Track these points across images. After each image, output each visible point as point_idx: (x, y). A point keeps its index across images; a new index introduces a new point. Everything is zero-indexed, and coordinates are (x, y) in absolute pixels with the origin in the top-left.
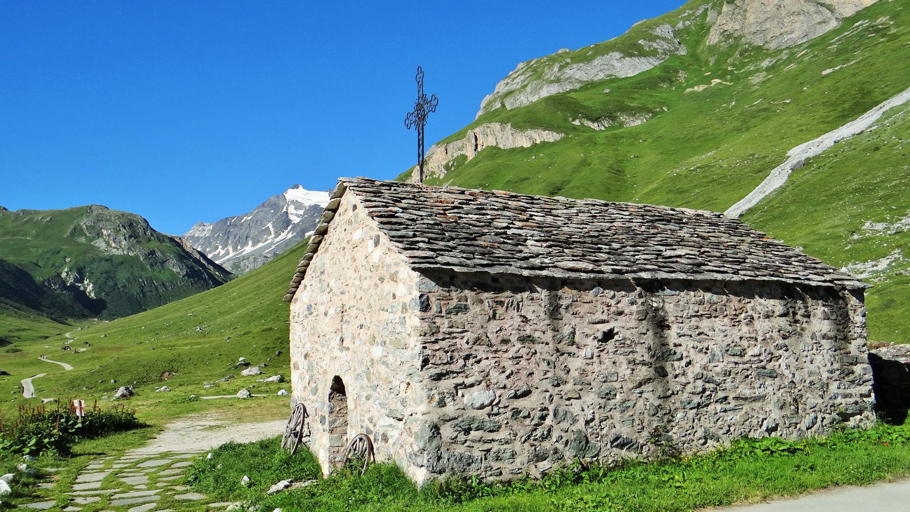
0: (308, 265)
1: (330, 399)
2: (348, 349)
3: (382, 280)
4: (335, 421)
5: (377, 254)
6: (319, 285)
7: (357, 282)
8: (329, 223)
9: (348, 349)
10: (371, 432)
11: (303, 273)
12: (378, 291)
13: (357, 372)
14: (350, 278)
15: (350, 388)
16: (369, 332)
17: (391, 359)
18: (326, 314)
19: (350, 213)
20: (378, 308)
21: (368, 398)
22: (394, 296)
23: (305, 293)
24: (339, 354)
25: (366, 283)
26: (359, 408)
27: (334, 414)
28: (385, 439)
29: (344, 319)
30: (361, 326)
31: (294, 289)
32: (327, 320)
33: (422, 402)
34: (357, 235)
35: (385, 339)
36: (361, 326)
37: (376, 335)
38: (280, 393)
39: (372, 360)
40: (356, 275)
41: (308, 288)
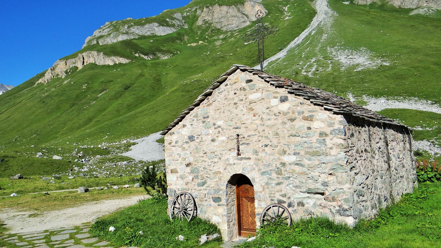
0: (188, 113)
1: (227, 187)
2: (249, 158)
3: (292, 120)
4: (228, 199)
5: (285, 107)
6: (201, 124)
7: (258, 122)
8: (213, 89)
9: (249, 158)
10: (284, 202)
11: (183, 118)
12: (287, 126)
13: (262, 171)
14: (247, 119)
15: (257, 180)
16: (277, 149)
17: (306, 162)
18: (213, 140)
19: (244, 84)
20: (288, 135)
21: (279, 184)
22: (309, 128)
23: (185, 129)
24: (236, 161)
25: (269, 123)
26: (267, 191)
27: (228, 195)
28: (301, 204)
29: (241, 143)
30: (266, 146)
31: (171, 127)
32: (216, 144)
33: (346, 182)
34: (253, 97)
35: (298, 151)
36: (266, 146)
37: (286, 149)
38: (12, 195)
39: (284, 164)
40: (255, 118)
41: (188, 126)
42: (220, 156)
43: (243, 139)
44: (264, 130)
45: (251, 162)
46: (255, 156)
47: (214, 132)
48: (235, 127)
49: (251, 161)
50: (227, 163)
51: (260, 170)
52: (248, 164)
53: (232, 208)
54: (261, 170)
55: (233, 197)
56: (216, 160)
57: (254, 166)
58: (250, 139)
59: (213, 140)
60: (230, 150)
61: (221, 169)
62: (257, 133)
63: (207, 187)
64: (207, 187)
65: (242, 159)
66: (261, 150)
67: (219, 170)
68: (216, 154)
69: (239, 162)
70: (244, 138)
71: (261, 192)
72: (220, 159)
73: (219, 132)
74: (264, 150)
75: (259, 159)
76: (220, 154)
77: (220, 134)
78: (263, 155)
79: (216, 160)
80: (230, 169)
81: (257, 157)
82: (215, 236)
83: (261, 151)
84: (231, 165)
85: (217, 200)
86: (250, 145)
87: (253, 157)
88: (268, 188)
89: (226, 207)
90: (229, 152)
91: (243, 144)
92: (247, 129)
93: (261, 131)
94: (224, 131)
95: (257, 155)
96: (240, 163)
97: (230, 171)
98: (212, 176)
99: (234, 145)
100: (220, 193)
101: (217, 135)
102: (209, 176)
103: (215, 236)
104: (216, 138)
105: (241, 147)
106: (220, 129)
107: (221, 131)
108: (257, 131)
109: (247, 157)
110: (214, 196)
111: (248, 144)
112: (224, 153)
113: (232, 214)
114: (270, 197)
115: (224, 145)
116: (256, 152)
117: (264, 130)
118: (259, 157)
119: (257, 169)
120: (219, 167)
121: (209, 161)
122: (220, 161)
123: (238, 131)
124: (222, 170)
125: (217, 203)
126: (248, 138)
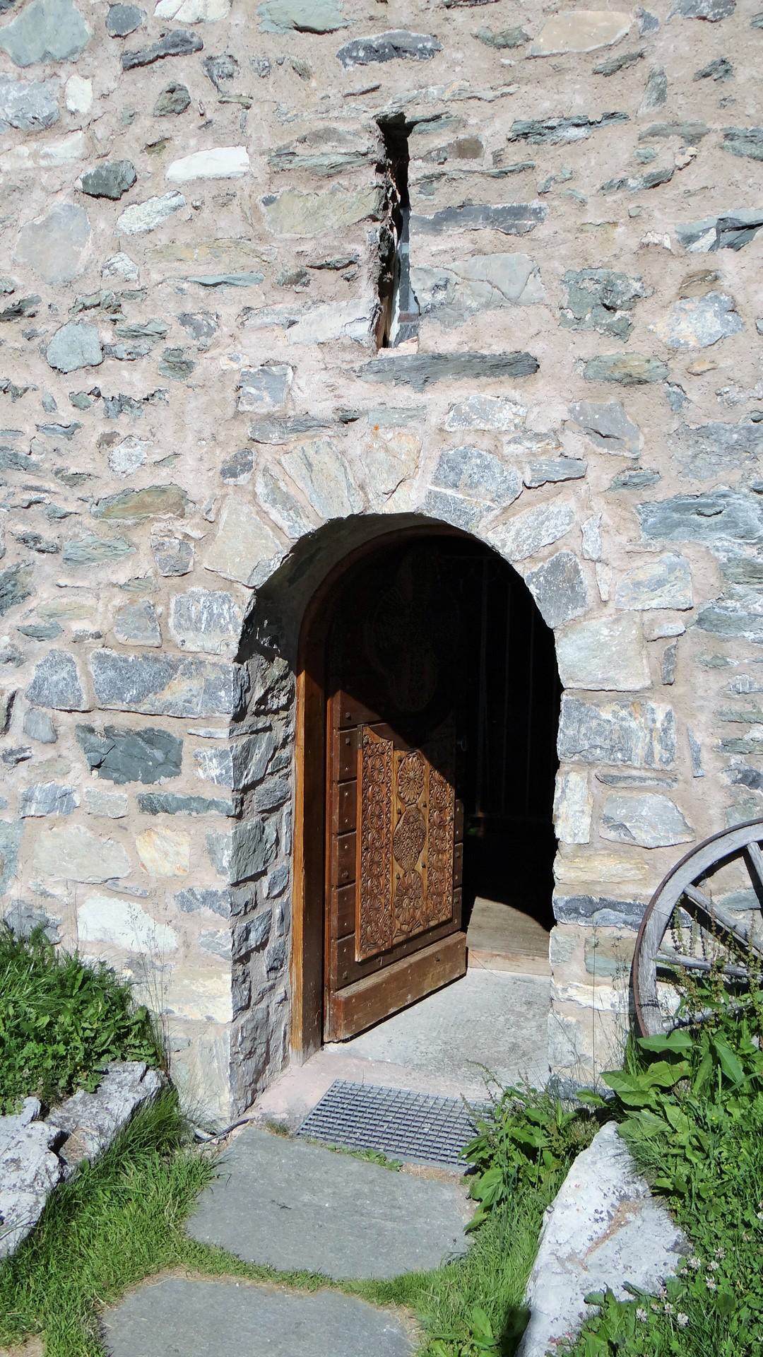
2: (520, 366)
4: (248, 750)
9: (520, 366)
13: (664, 492)
15: (601, 581)
24: (358, 394)
29: (421, 205)
42: (180, 337)
43: (454, 165)
44: (722, 69)
45: (545, 404)
46: (593, 344)
47: (117, 103)
48: (374, 37)
49: (541, 386)
50: (266, 405)
51: (632, 481)
52: (505, 416)
53: (270, 833)
54: (648, 482)
55: (279, 733)
56: (134, 380)
57: (575, 443)
58: (548, 161)
59: (106, 189)
60: (299, 278)
61: (189, 461)
62: (638, 102)
63: (35, 634)
64: (35, 634)
65: (430, 369)
66: (671, 276)
67: (162, 477)
68: (132, 317)
69: (404, 395)
70: (469, 149)
71: (633, 700)
72: (179, 365)
73: (176, 102)
74: (710, 278)
75: (637, 366)
76: (185, 319)
77: (189, 121)
78: (694, 325)
79: (134, 380)
80: (291, 464)
81: (611, 350)
82: (124, 1090)
83: (669, 288)
84: (305, 425)
85: (135, 756)
86: (543, 231)
87: (565, 350)
88: (718, 664)
89: (227, 829)
90: (287, 303)
91: (450, 215)
92: (507, 58)
93: (680, 73)
94: (235, 88)
95: (622, 332)
96: (418, 413)
97: (300, 489)
98: (85, 531)
99: (348, 231)
100: (167, 696)
101: (147, 129)
102: (49, 534)
103: (124, 1090)
104: (145, 164)
105: (421, 249)
106: (184, 70)
107: (201, 94)
108: (639, 72)
109: (497, 347)
110: (99, 721)
111: (518, 212)
112: (228, 312)
113: (265, 881)
114: (729, 745)
115: (229, 224)
116: (609, 303)
117: (722, 69)
118: (635, 353)
119: (601, 473)
120: (178, 445)
121: (59, 390)
122: (175, 387)
123: (401, 88)
124: (194, 477)
125: (141, 788)
126: (516, 155)
